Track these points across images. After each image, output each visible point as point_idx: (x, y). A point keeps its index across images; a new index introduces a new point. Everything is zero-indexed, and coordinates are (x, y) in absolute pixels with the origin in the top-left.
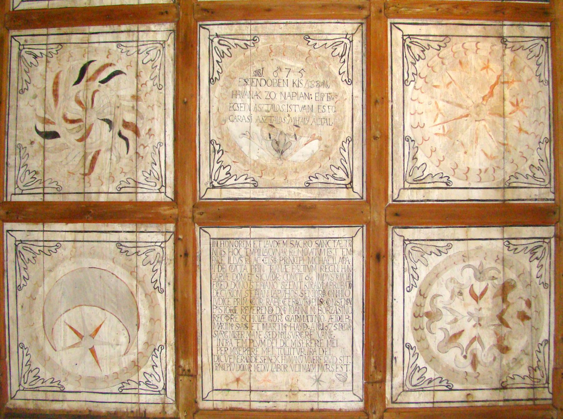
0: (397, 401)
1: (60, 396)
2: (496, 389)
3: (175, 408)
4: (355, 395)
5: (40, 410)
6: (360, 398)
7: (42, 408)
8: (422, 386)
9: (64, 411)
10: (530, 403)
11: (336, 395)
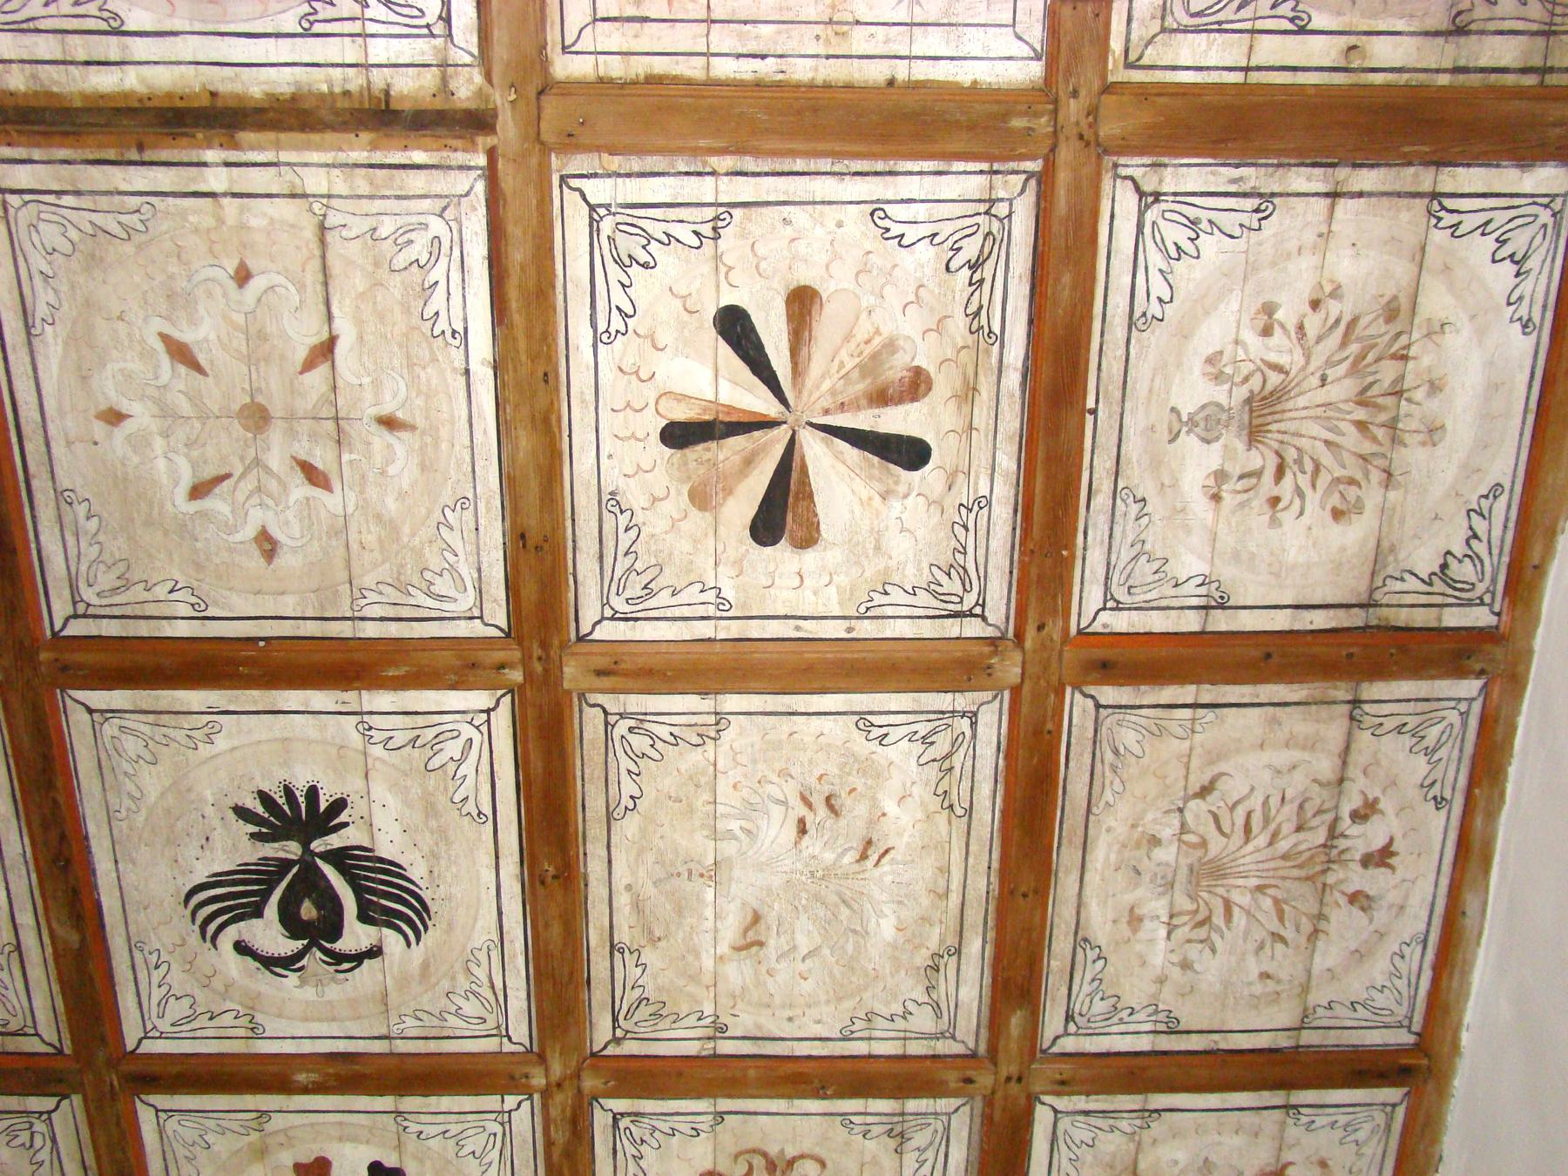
0: (1141, 63)
1: (111, 48)
2: (1437, 34)
3: (478, 79)
4: (1020, 38)
5: (50, 95)
6: (1034, 50)
7: (55, 89)
8: (1220, 17)
9: (126, 95)
10: (1530, 80)
11: (965, 39)
